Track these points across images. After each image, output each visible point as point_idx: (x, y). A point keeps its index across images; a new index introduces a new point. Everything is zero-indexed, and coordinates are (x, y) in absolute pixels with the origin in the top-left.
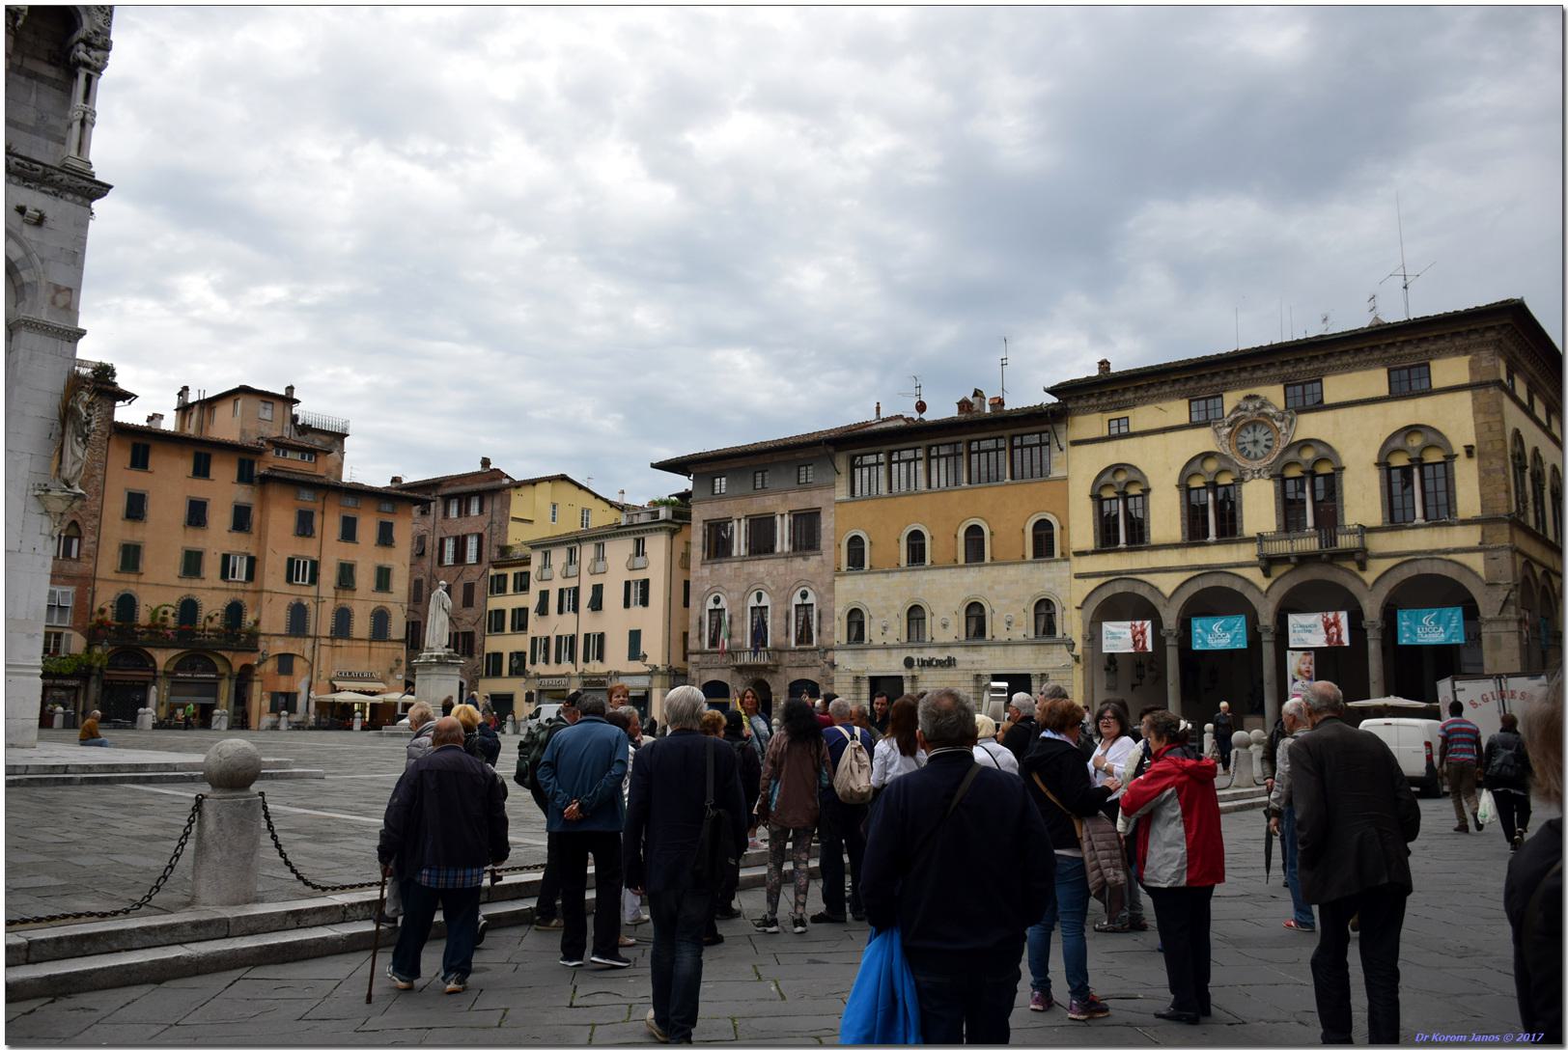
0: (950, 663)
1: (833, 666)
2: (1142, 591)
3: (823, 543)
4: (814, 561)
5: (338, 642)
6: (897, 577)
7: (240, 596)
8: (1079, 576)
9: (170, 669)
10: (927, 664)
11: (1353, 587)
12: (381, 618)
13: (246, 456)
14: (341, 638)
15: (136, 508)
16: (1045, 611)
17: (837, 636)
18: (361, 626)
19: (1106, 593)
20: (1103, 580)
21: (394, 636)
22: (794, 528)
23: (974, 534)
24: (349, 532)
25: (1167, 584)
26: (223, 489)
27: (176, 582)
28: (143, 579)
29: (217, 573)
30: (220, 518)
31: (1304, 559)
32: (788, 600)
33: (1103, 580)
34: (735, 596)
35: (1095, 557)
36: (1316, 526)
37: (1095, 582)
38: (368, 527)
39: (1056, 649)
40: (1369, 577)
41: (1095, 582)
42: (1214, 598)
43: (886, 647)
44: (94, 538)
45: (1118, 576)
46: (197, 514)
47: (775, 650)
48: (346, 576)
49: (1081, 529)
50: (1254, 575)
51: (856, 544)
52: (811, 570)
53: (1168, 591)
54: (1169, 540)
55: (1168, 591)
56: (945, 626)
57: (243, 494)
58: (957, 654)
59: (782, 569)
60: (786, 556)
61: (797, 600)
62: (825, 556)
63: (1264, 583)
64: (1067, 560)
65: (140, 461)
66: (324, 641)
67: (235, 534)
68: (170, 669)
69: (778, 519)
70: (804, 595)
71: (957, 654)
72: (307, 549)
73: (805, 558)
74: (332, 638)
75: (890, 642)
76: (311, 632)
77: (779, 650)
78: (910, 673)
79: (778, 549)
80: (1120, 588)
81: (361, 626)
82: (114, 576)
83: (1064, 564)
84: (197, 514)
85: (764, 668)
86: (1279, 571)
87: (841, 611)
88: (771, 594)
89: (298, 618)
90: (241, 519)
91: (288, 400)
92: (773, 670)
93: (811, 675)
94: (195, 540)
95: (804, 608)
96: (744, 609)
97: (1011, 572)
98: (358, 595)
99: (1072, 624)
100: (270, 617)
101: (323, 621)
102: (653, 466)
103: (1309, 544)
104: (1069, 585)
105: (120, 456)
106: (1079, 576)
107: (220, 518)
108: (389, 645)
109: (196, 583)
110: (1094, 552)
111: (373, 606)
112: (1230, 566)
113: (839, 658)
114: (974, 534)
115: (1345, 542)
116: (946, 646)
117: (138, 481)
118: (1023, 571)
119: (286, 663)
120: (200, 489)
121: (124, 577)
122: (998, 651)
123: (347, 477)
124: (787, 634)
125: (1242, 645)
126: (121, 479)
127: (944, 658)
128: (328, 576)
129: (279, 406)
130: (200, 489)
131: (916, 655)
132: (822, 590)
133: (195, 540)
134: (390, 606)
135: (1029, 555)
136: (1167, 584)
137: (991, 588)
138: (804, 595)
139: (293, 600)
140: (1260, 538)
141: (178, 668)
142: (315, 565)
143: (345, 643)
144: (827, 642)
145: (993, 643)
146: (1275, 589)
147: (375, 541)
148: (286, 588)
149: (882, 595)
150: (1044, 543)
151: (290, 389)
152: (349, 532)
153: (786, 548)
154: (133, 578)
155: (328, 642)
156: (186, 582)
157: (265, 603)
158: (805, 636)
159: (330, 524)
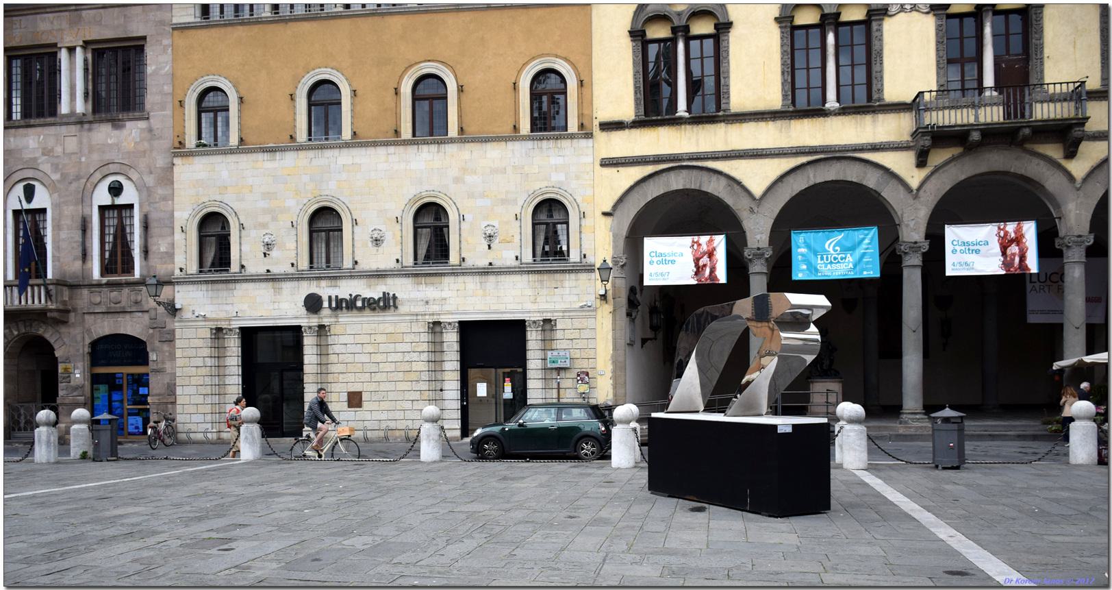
0: (386, 303)
1: (173, 310)
2: (715, 187)
3: (152, 98)
4: (133, 130)
6: (289, 160)
8: (608, 163)
10: (347, 305)
11: (1052, 182)
16: (550, 215)
17: (179, 260)
19: (655, 190)
20: (650, 169)
22: (94, 73)
23: (429, 94)
25: (757, 176)
31: (993, 136)
32: (84, 197)
33: (650, 169)
35: (636, 133)
36: (998, 86)
37: (638, 172)
39: (569, 280)
40: (1079, 167)
41: (638, 172)
42: (832, 200)
43: (270, 278)
45: (677, 163)
47: (59, 283)
49: (613, 86)
50: (902, 163)
51: (210, 103)
52: (129, 145)
53: (757, 187)
54: (761, 106)
55: (757, 187)
56: (377, 242)
58: (400, 288)
59: (72, 144)
60: (80, 121)
61: (102, 197)
62: (155, 122)
63: (914, 177)
64: (589, 136)
69: (63, 55)
70: (116, 190)
71: (400, 288)
73: (117, 124)
75: (276, 270)
77: (71, 285)
78: (314, 321)
79: (64, 108)
80: (677, 182)
83: (584, 143)
85: (40, 316)
86: (938, 157)
87: (186, 216)
88: (51, 187)
92: (61, 318)
93: (132, 326)
95: (116, 213)
97: (494, 152)
99: (595, 239)
103: (993, 115)
104: (593, 178)
106: (608, 163)
110: (637, 124)
112: (875, 148)
113: (184, 297)
114: (429, 94)
115: (1042, 112)
116: (380, 275)
118: (515, 152)
122: (471, 283)
124: (85, 256)
125: (872, 271)
127: (376, 295)
131: (325, 291)
132: (150, 180)
135: (525, 126)
136: (757, 176)
137: (457, 180)
138: (116, 190)
140: (914, 106)
144: (161, 269)
145: (462, 271)
146: (928, 186)
149: (265, 193)
150: (548, 109)
153: (80, 107)
158: (118, 259)
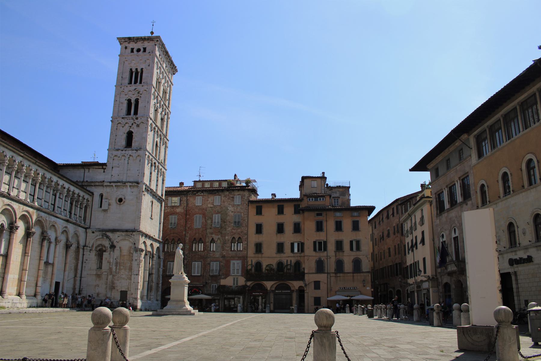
5: (338, 275)
7: (299, 258)
9: (273, 289)
12: (357, 263)
13: (296, 203)
14: (340, 273)
15: (259, 229)
18: (348, 266)
21: (364, 270)
24: (339, 227)
26: (289, 217)
27: (275, 255)
28: (263, 256)
29: (290, 251)
30: (289, 228)
34: (447, 232)
38: (347, 224)
44: (246, 242)
46: (280, 229)
48: (339, 245)
57: (297, 218)
65: (259, 212)
66: (332, 275)
67: (295, 234)
68: (273, 289)
72: (321, 237)
74: (335, 273)
76: (326, 271)
81: (348, 266)
82: (253, 255)
84: (280, 229)
89: (320, 267)
90: (297, 228)
91: (323, 178)
94: (281, 238)
96: (451, 239)
98: (345, 254)
100: (309, 266)
101: (331, 266)
102: (411, 170)
105: (252, 211)
107: (289, 228)
108: (362, 274)
109: (282, 255)
111: (352, 258)
117: (259, 219)
119: (317, 285)
120: (281, 219)
121: (257, 255)
123: (353, 204)
126: (254, 219)
128: (331, 247)
129: (319, 180)
130: (281, 219)
133: (281, 238)
134: (360, 257)
139: (317, 258)
141: (277, 288)
142: (325, 243)
143: (341, 275)
147: (351, 230)
148: (314, 253)
151: (323, 173)
152: (339, 227)
154: (260, 255)
155: (334, 275)
156: (278, 255)
157: (306, 261)
159: (330, 225)
